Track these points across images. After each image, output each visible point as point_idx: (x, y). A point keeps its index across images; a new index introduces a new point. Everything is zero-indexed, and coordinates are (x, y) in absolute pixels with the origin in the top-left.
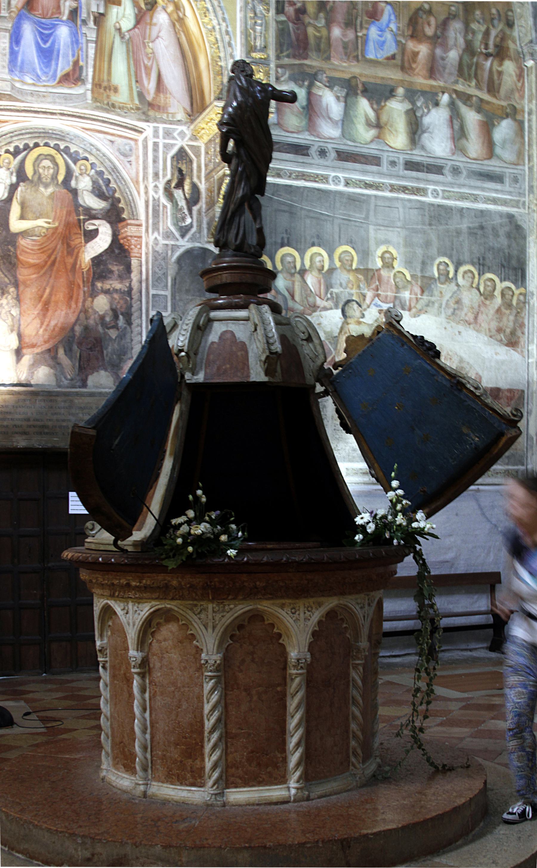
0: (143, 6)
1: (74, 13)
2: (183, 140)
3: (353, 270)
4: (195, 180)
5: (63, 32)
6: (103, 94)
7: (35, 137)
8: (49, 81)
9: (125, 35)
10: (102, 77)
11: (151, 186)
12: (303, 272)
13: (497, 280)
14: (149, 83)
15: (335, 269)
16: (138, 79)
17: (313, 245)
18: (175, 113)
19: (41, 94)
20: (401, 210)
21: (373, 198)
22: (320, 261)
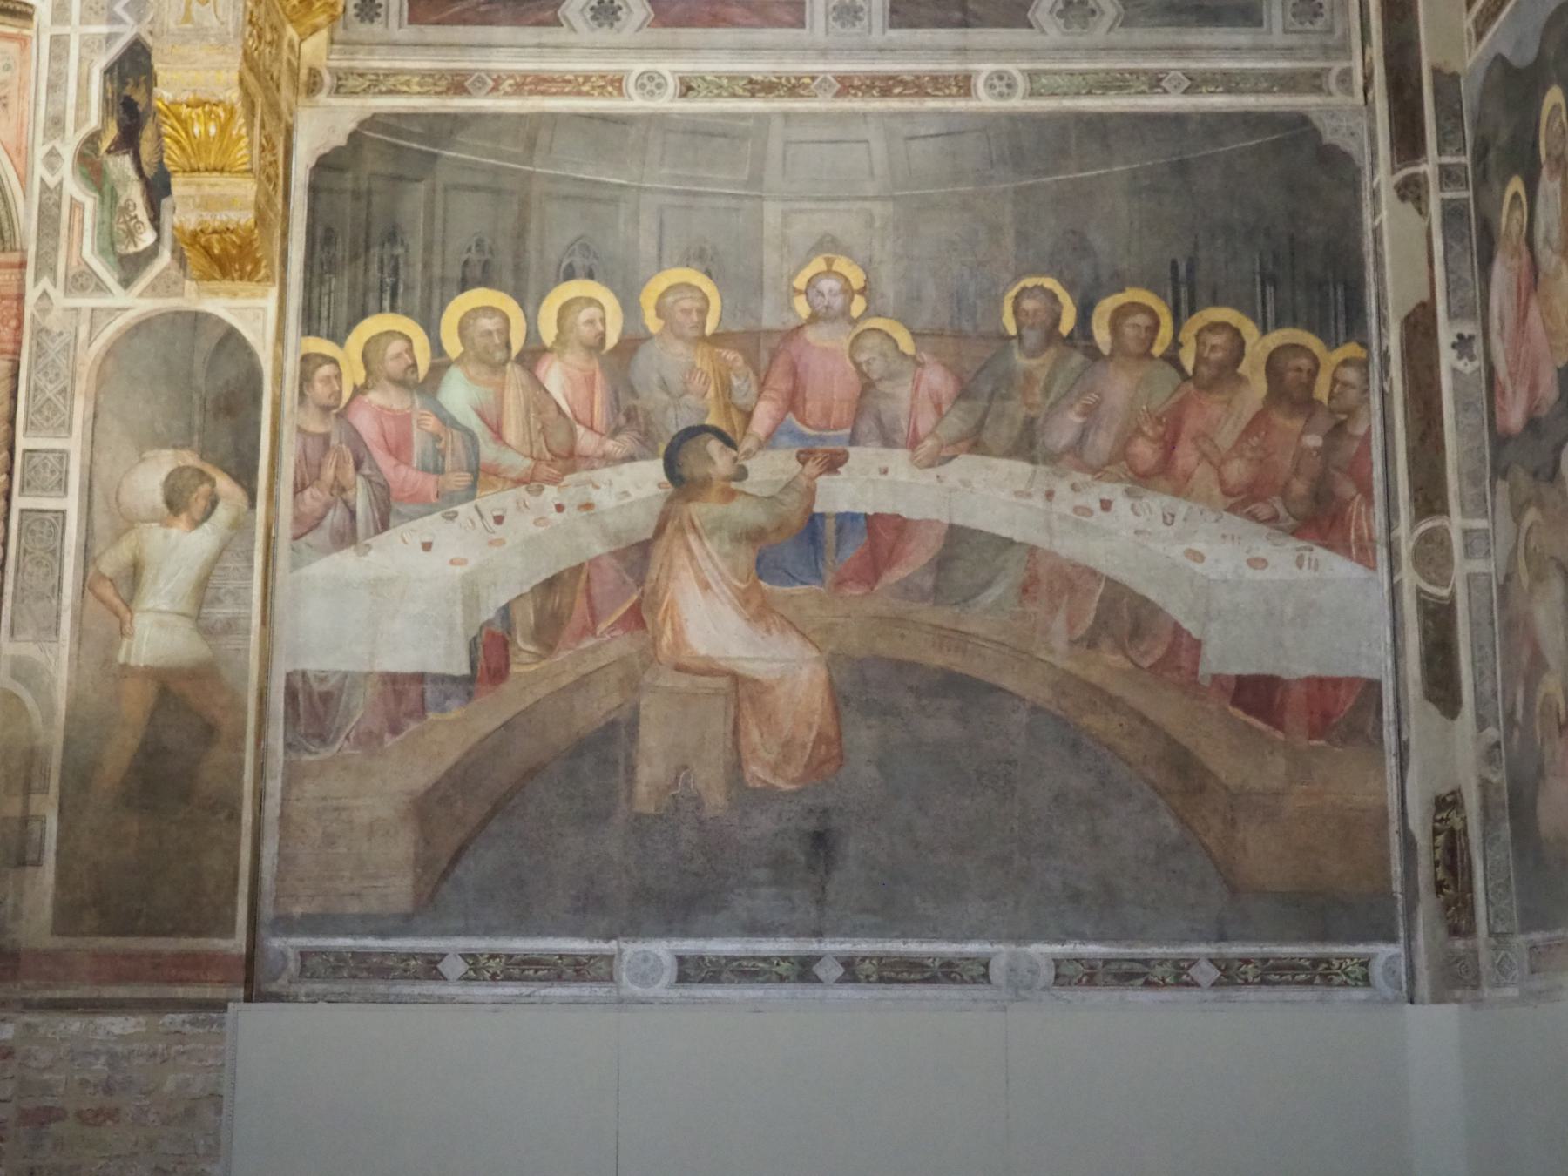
3: (703, 338)
12: (532, 355)
13: (1249, 330)
15: (649, 337)
17: (570, 275)
20: (878, 147)
21: (777, 124)
22: (591, 322)
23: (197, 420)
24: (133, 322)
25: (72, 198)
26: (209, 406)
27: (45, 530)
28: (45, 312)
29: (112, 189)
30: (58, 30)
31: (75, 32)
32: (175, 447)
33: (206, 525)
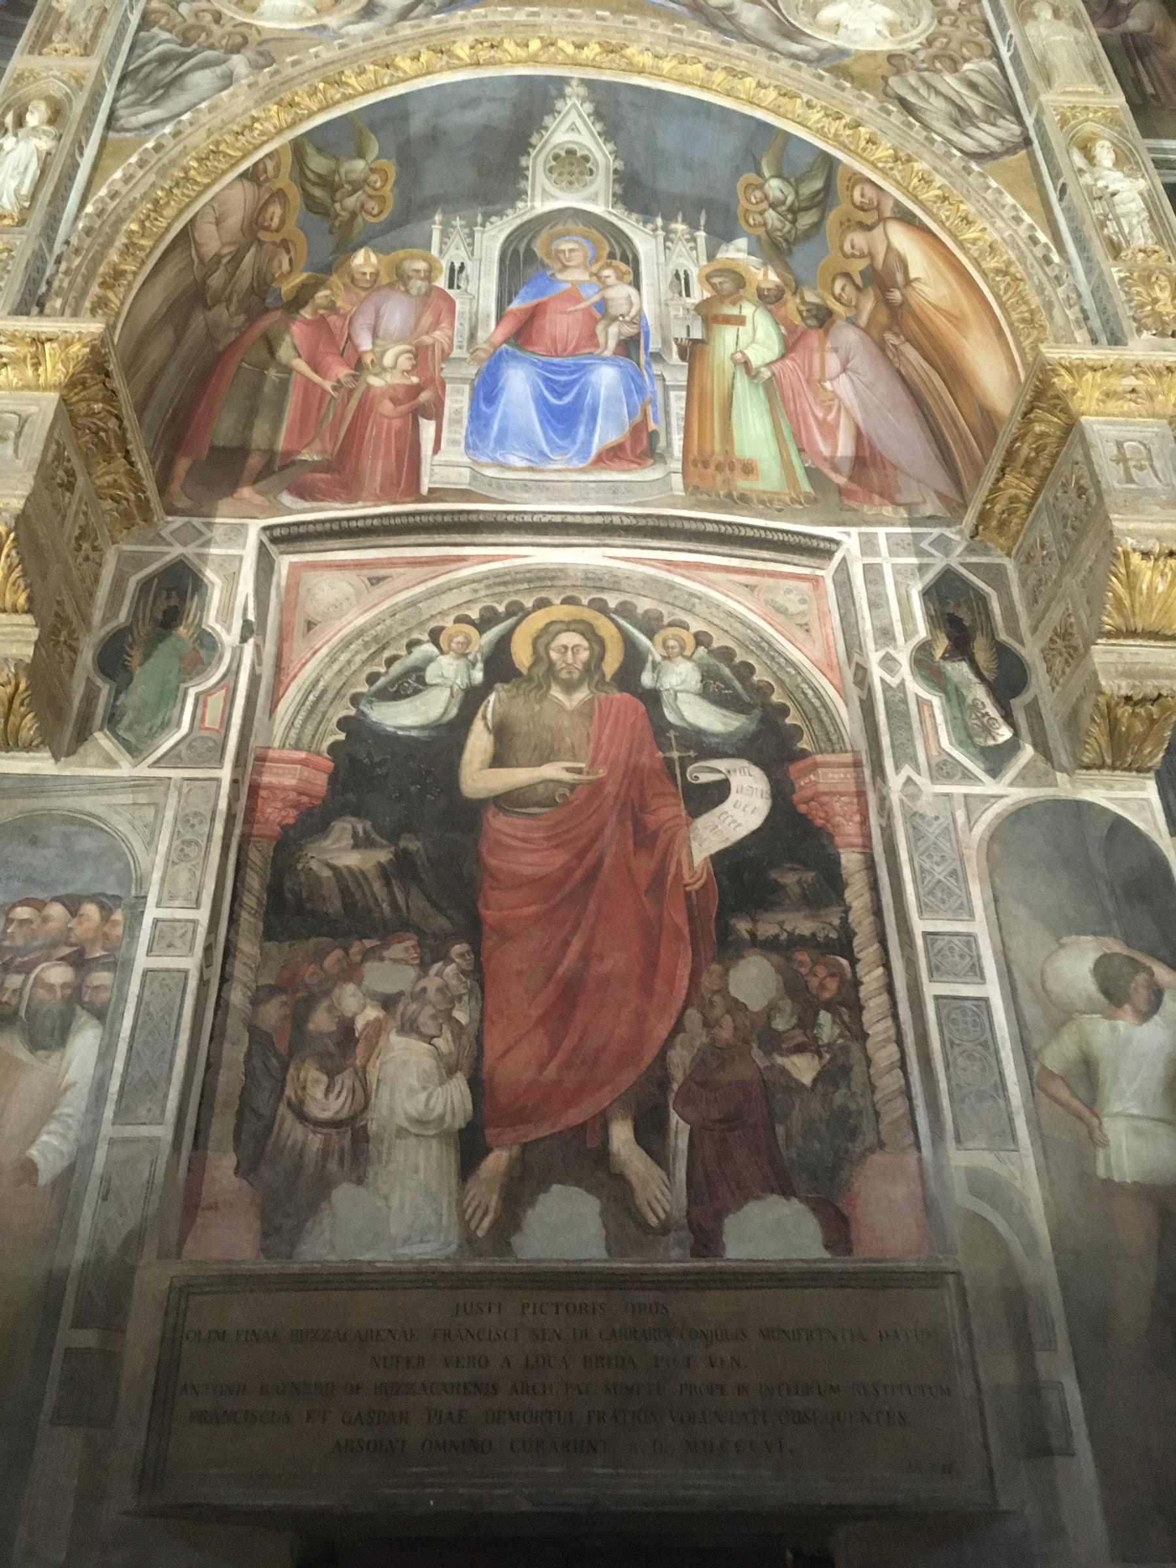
0: (797, 320)
1: (629, 346)
2: (947, 555)
4: (1003, 636)
5: (606, 378)
6: (714, 478)
9: (758, 373)
10: (708, 447)
11: (874, 658)
18: (918, 504)
23: (1111, 907)
24: (1012, 809)
25: (917, 696)
26: (1119, 892)
27: (969, 1019)
28: (914, 797)
29: (957, 690)
30: (870, 560)
31: (887, 563)
32: (1094, 934)
33: (1156, 1017)
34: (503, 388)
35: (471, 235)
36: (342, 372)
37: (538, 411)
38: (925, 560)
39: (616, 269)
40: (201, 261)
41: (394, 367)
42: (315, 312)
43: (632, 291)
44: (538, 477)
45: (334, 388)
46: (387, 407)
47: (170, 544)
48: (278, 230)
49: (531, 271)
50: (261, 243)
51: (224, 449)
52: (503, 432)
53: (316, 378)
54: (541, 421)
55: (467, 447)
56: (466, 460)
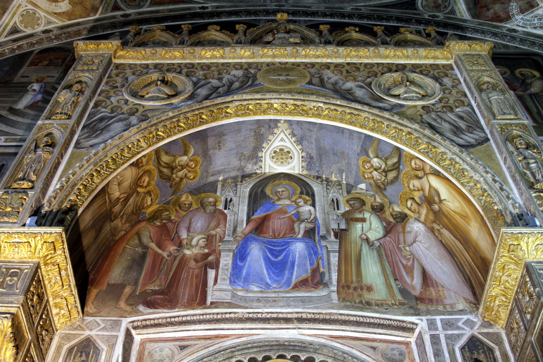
0: (391, 219)
1: (310, 233)
2: (472, 329)
5: (299, 248)
6: (353, 294)
7: (265, 351)
8: (281, 287)
14: (412, 278)
16: (398, 277)
19: (270, 299)
34: (248, 254)
35: (236, 185)
36: (172, 248)
37: (266, 264)
38: (461, 332)
39: (304, 199)
40: (110, 201)
41: (196, 245)
42: (161, 222)
43: (312, 208)
44: (265, 295)
45: (168, 256)
46: (192, 264)
47: (83, 330)
48: (146, 187)
49: (264, 201)
50: (138, 193)
51: (114, 285)
52: (248, 274)
53: (160, 251)
54: (267, 269)
55: (231, 281)
56: (230, 287)
